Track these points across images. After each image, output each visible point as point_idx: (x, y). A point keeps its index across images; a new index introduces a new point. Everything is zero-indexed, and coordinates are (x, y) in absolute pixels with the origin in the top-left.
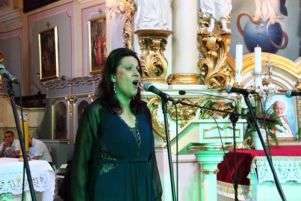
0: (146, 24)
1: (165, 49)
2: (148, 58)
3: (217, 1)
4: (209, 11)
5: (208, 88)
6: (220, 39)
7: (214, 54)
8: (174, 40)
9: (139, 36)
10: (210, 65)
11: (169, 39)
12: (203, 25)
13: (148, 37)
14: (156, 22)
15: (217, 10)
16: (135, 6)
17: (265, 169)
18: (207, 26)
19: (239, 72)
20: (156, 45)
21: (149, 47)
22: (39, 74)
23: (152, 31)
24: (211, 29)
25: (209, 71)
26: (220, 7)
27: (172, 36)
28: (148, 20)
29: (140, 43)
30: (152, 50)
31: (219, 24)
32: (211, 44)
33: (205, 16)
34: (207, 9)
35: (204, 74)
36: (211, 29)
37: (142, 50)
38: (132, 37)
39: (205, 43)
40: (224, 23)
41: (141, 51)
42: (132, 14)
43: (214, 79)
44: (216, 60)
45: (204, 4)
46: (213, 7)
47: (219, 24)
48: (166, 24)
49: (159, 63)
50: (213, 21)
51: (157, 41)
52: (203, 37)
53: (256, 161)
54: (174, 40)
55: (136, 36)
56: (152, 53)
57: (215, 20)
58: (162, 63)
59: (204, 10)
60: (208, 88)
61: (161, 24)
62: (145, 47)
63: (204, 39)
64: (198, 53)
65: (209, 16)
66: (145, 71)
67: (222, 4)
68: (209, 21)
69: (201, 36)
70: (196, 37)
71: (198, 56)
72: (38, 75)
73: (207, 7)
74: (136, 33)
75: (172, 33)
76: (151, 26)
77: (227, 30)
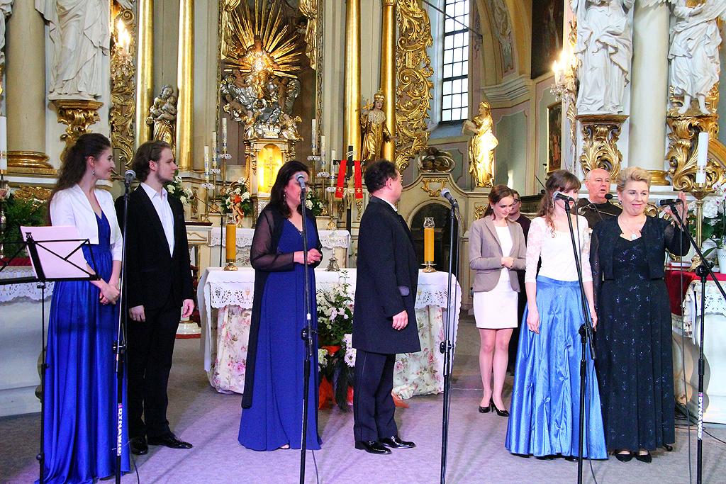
0: (589, 107)
1: (618, 139)
2: (591, 151)
3: (693, 72)
4: (681, 86)
5: (674, 190)
6: (696, 123)
7: (687, 143)
8: (631, 126)
9: (583, 122)
10: (681, 158)
11: (624, 127)
12: (675, 105)
13: (591, 124)
14: (601, 104)
15: (694, 84)
16: (577, 84)
17: (710, 297)
18: (681, 105)
19: (702, 169)
20: (601, 133)
21: (594, 137)
22: (546, 165)
23: (593, 116)
24: (682, 111)
25: (679, 167)
26: (696, 79)
27: (630, 120)
28: (591, 102)
29: (582, 132)
30: (597, 140)
31: (694, 102)
32: (681, 130)
33: (675, 92)
34: (679, 83)
35: (673, 170)
36: (682, 111)
37: (585, 139)
38: (575, 123)
39: (675, 128)
40: (702, 100)
41: (584, 142)
42: (576, 96)
43: (686, 178)
44: (691, 151)
45: (676, 76)
46: (687, 78)
47: (694, 102)
48: (617, 106)
49: (605, 157)
50: (687, 99)
51: (602, 129)
52: (673, 120)
53: (694, 286)
54: (631, 126)
55: (578, 122)
56: (597, 144)
57: (692, 97)
58: (610, 157)
59: (675, 84)
60: (674, 190)
61: (610, 106)
62: (589, 137)
63: (673, 124)
64: (668, 142)
65: (680, 91)
66: (587, 167)
67: (700, 76)
68: (683, 98)
69: (671, 120)
70: (661, 119)
71: (667, 145)
72: (545, 167)
73: (679, 81)
74: (577, 118)
75: (627, 117)
76: (594, 111)
77: (704, 111)
